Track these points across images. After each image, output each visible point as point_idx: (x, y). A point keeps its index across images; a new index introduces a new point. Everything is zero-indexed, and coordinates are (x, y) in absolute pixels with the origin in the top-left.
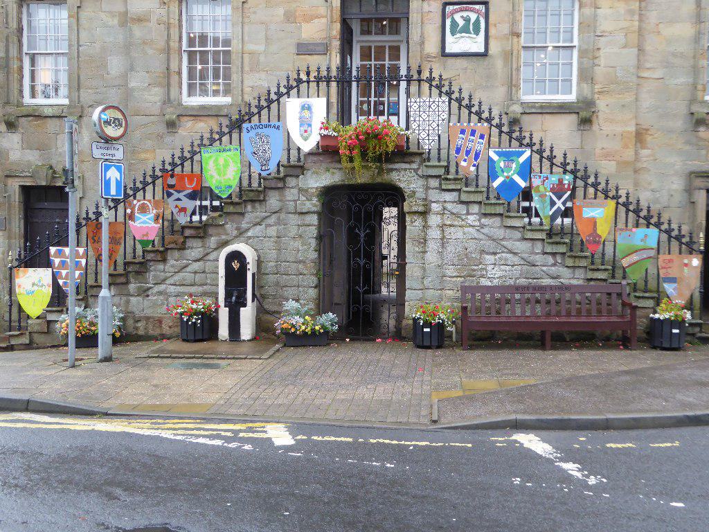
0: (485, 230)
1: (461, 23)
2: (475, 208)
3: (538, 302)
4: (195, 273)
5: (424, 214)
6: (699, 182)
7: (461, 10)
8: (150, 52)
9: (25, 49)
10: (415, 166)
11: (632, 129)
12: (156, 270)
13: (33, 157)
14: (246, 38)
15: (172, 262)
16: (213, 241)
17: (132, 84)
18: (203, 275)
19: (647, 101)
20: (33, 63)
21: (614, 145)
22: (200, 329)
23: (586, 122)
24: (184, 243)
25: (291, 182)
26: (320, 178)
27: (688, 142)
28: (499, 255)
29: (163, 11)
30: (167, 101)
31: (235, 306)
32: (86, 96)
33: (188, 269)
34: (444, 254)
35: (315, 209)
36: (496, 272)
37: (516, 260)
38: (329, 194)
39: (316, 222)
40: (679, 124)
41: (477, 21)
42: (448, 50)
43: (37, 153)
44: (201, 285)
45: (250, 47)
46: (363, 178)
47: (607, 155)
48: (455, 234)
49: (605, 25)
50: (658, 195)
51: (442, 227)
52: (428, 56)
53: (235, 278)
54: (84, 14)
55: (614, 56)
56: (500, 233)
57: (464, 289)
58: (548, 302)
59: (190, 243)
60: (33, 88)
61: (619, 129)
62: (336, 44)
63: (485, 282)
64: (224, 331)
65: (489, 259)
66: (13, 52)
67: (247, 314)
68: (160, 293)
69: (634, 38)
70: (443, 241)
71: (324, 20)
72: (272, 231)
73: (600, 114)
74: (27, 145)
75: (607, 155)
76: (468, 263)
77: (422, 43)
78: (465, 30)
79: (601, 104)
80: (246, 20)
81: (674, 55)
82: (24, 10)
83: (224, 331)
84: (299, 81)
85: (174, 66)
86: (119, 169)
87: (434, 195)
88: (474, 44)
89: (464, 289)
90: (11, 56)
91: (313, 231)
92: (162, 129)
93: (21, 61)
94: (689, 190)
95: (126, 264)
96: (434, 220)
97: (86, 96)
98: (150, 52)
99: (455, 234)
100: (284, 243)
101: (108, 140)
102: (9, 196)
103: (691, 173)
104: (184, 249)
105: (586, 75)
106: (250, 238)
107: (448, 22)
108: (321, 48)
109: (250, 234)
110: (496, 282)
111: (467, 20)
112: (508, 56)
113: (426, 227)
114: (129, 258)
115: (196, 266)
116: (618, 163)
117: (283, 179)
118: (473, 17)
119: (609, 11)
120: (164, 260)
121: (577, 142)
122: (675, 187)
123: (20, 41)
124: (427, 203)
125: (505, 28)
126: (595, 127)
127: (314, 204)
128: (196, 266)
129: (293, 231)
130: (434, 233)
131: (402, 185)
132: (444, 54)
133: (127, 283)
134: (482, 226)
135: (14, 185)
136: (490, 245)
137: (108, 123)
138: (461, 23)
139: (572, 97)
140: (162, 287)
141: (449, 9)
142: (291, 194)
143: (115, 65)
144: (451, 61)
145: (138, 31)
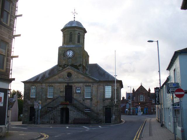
6: (104, 107)
13: (31, 103)
16: (50, 113)
17: (43, 95)
19: (98, 98)
23: (91, 100)
27: (103, 102)
34: (73, 114)
40: (102, 101)
49: (93, 90)
55: (94, 93)
62: (64, 91)
75: (94, 104)
88: (79, 92)
94: (103, 108)
96: (72, 111)
100: (57, 113)
105: (92, 95)
125: (83, 90)
132: (76, 93)
139: (90, 97)
143: (41, 93)
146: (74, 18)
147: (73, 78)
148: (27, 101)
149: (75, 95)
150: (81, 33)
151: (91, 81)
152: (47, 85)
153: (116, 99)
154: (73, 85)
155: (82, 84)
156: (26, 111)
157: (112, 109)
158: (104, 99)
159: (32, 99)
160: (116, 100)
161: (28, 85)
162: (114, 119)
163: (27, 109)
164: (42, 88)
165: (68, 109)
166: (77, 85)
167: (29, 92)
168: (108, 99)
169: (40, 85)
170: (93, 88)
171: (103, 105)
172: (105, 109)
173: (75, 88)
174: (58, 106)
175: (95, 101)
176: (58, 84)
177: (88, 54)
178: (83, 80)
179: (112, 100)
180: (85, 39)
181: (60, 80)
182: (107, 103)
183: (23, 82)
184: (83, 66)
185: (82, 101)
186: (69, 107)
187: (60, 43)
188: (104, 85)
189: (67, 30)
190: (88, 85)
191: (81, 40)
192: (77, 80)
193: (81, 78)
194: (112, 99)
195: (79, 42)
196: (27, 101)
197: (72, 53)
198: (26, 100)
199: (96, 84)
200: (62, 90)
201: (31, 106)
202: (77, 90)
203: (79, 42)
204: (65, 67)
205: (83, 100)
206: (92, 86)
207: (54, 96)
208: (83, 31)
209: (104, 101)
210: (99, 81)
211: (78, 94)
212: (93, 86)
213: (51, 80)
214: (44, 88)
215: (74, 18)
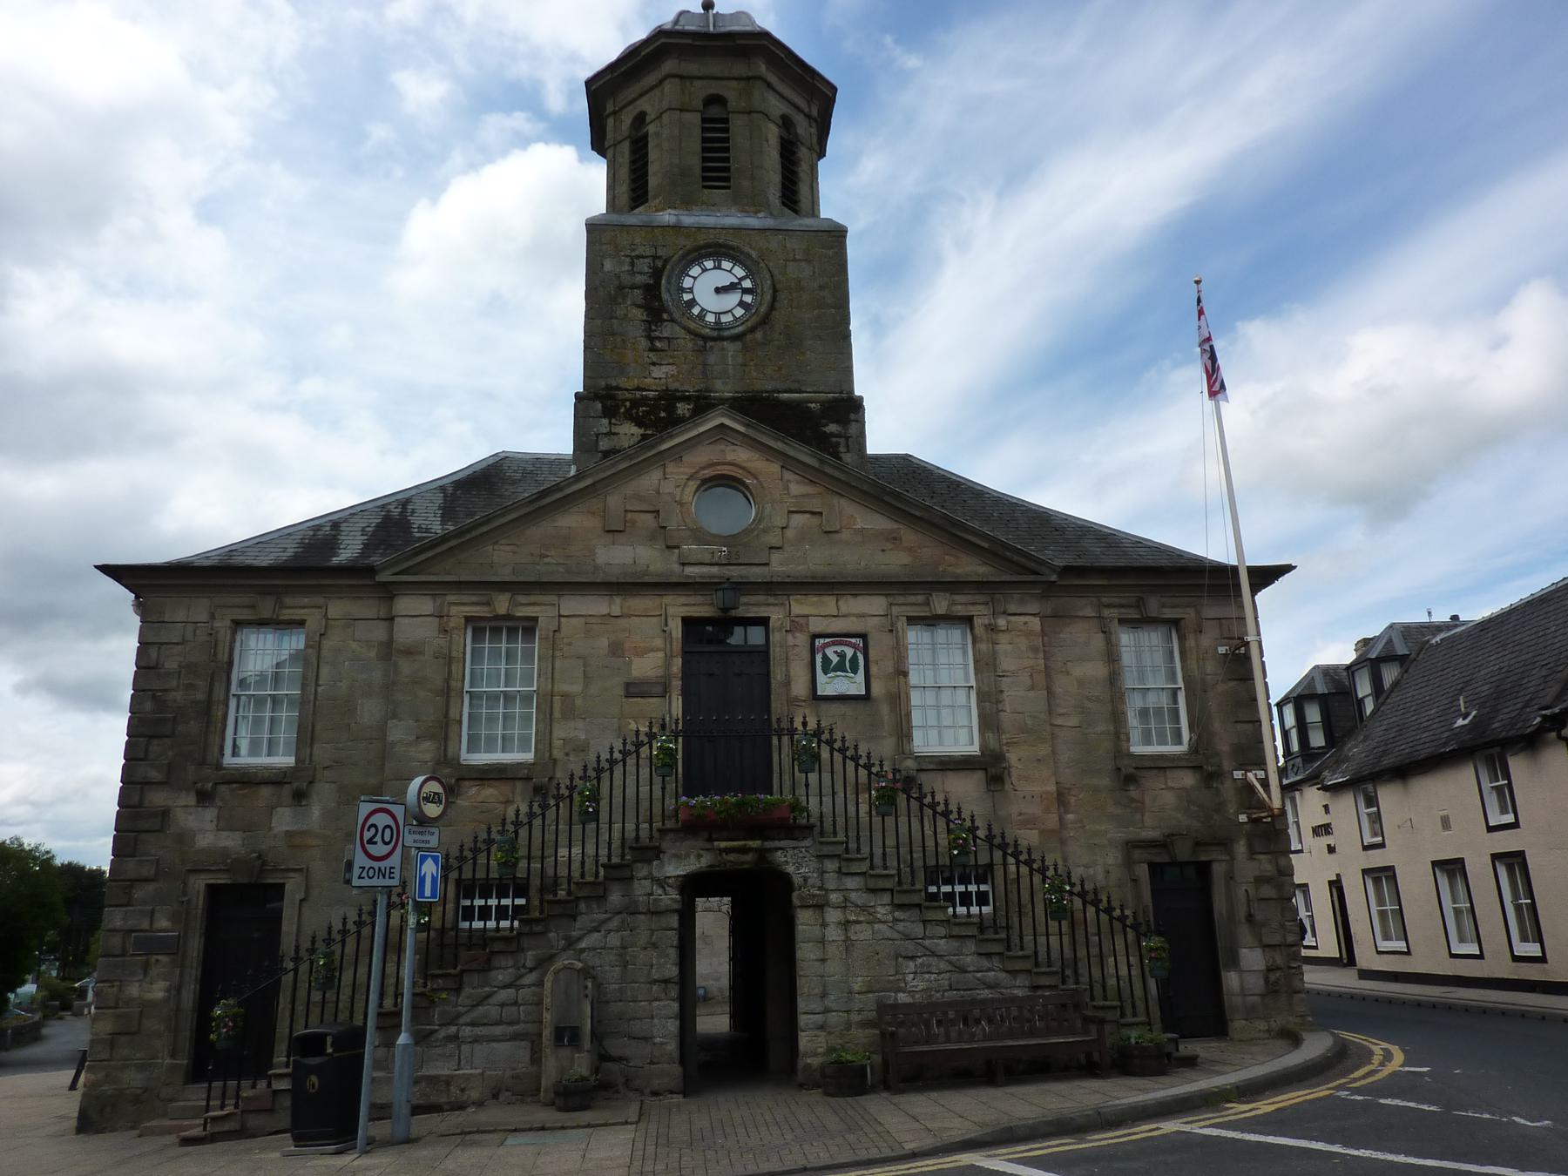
0: (900, 926)
1: (835, 659)
2: (886, 898)
4: (503, 1005)
6: (1137, 854)
7: (834, 644)
8: (422, 694)
10: (807, 843)
11: (1052, 788)
13: (231, 841)
14: (557, 676)
15: (467, 990)
16: (530, 958)
18: (514, 1008)
21: (1035, 810)
24: (489, 960)
25: (642, 870)
28: (919, 961)
32: (322, 753)
33: (493, 1000)
35: (676, 906)
36: (917, 984)
37: (943, 965)
39: (675, 924)
40: (1106, 782)
41: (854, 659)
43: (238, 835)
44: (511, 1023)
48: (862, 933)
49: (1007, 664)
50: (1091, 871)
51: (846, 925)
52: (796, 699)
54: (327, 644)
56: (918, 930)
61: (1036, 789)
62: (677, 684)
63: (903, 998)
71: (661, 654)
72: (614, 940)
74: (225, 824)
75: (1029, 822)
78: (840, 667)
79: (1013, 757)
80: (558, 653)
81: (1089, 699)
85: (453, 713)
86: (435, 860)
88: (853, 685)
90: (215, 698)
93: (227, 706)
94: (1129, 863)
96: (833, 916)
97: (322, 753)
98: (422, 694)
102: (189, 902)
103: (1127, 843)
104: (490, 970)
106: (583, 950)
108: (659, 689)
109: (583, 945)
115: (504, 995)
116: (1041, 832)
117: (628, 866)
118: (849, 652)
119: (1009, 648)
122: (1110, 860)
125: (889, 666)
126: (1008, 787)
127: (671, 897)
128: (504, 995)
129: (643, 939)
131: (790, 869)
134: (896, 920)
135: (199, 883)
136: (910, 947)
137: (427, 799)
138: (835, 659)
140: (453, 1029)
141: (819, 642)
142: (641, 888)
143: (369, 711)
144: (824, 706)
145: (406, 667)
148: (165, 813)
151: (971, 567)
152: (462, 608)
154: (776, 615)
156: (150, 945)
157: (1218, 870)
158: (1131, 774)
159: (248, 780)
161: (191, 612)
162: (1256, 983)
163: (164, 923)
164: (388, 650)
165: (784, 883)
166: (819, 612)
167: (209, 702)
168: (1160, 765)
169: (366, 608)
170: (1004, 645)
171: (1119, 835)
172: (1143, 871)
173: (801, 639)
174: (648, 852)
175: (1031, 786)
176: (597, 606)
178: (893, 561)
181: (617, 557)
186: (795, 861)
188: (1106, 612)
189: (669, 66)
192: (816, 560)
196: (165, 813)
198: (158, 798)
199: (1033, 607)
200: (646, 667)
201: (222, 880)
202: (815, 676)
204: (675, 422)
206: (992, 628)
207: (545, 741)
209: (1134, 792)
210: (1067, 571)
213: (502, 559)
214: (410, 652)
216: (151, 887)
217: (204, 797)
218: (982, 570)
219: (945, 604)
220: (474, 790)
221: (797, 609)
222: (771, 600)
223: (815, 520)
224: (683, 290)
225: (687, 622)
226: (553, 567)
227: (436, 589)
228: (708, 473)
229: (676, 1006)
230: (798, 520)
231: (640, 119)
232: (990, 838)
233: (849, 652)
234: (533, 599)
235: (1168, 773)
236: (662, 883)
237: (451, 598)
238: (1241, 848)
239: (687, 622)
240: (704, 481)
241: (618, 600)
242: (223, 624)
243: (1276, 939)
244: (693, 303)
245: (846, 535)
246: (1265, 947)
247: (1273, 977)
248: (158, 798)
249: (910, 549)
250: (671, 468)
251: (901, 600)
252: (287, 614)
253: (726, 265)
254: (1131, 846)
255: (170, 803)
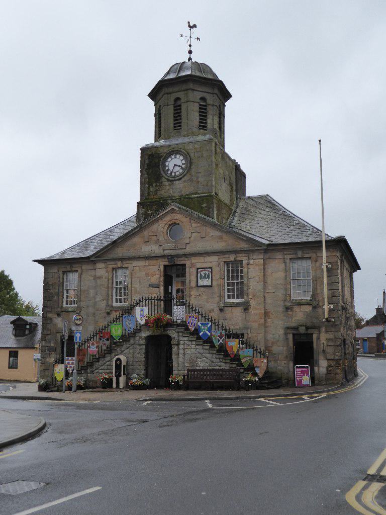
1: (203, 275)
2: (194, 343)
3: (215, 375)
5: (178, 345)
6: (289, 331)
9: (65, 288)
10: (174, 329)
11: (263, 312)
12: (96, 365)
17: (97, 300)
20: (67, 293)
22: (107, 385)
23: (246, 310)
25: (137, 334)
26: (145, 334)
29: (107, 274)
30: (108, 305)
31: (118, 376)
34: (187, 357)
35: (144, 343)
36: (201, 365)
37: (208, 360)
38: (148, 338)
40: (281, 309)
41: (209, 275)
42: (199, 285)
45: (134, 286)
46: (158, 333)
47: (255, 321)
50: (275, 336)
51: (184, 349)
53: (118, 367)
54: (83, 276)
56: (202, 351)
57: (189, 370)
58: (218, 375)
59: (107, 355)
60: (67, 301)
63: (198, 368)
64: (114, 385)
65: (199, 360)
66: (61, 289)
67: (122, 379)
68: (97, 372)
69: (262, 279)
70: (184, 354)
71: (158, 276)
72: (131, 351)
73: (252, 306)
75: (255, 321)
76: (193, 361)
77: (190, 283)
78: (205, 277)
79: (251, 303)
82: (65, 275)
83: (114, 385)
84: (140, 301)
85: (110, 293)
86: (80, 333)
87: (181, 338)
88: (207, 282)
89: (189, 370)
91: (144, 351)
92: (105, 315)
94: (286, 334)
95: (87, 363)
96: (181, 347)
99: (188, 352)
100: (133, 355)
101: (78, 325)
107: (199, 275)
109: (125, 352)
110: (201, 368)
111: (205, 274)
112: (219, 286)
113: (178, 349)
114: (88, 361)
115: (108, 363)
118: (207, 273)
120: (98, 361)
121: (244, 316)
123: (63, 286)
124: (179, 341)
126: (250, 311)
127: (143, 342)
128: (108, 363)
130: (181, 351)
132: (197, 286)
133: (88, 369)
134: (196, 349)
136: (199, 355)
138: (203, 275)
140: (98, 370)
142: (137, 338)
143: (92, 293)
145: (99, 282)
146: (190, 52)
147: (187, 241)
148: (51, 319)
149: (194, 293)
150: (210, 99)
151: (244, 245)
153: (329, 303)
154: (188, 263)
155: (214, 259)
157: (315, 336)
160: (326, 307)
161: (54, 269)
162: (323, 371)
164: (96, 278)
165: (169, 338)
166: (199, 262)
168: (299, 304)
169: (90, 267)
172: (290, 337)
173: (194, 270)
177: (242, 168)
178: (220, 246)
179: (314, 308)
180: (226, 119)
181: (147, 249)
182: (300, 316)
183: (41, 262)
184: (220, 202)
185: (215, 315)
187: (145, 133)
188: (286, 256)
189: (164, 90)
190: (233, 259)
191: (209, 121)
192: (199, 246)
193: (213, 240)
194: (314, 303)
195: (203, 125)
196: (51, 319)
197: (184, 162)
198: (50, 315)
203: (203, 125)
205: (221, 310)
206: (248, 264)
208: (216, 91)
209: (290, 312)
210: (269, 245)
211: (202, 289)
212: (251, 262)
213: (120, 252)
214: (99, 278)
215: (190, 52)
216: (49, 336)
217: (59, 315)
218: (246, 246)
219: (231, 258)
220: (114, 313)
221: (193, 261)
222: (186, 259)
223: (199, 234)
224: (166, 166)
225: (165, 266)
226: (132, 253)
227: (105, 261)
228: (170, 223)
229: (144, 368)
230: (194, 234)
231: (160, 106)
232: (223, 327)
233: (207, 273)
234: (127, 262)
235: (302, 306)
236: (141, 337)
237: (108, 263)
238: (323, 329)
239: (165, 266)
240: (170, 225)
241: (147, 261)
242: (61, 273)
243: (332, 358)
244: (168, 170)
245: (207, 238)
246: (328, 360)
247: (330, 369)
248: (50, 315)
249: (226, 241)
250: (160, 222)
251: (222, 256)
252: (74, 269)
253: (178, 156)
254: (288, 328)
255: (52, 317)
